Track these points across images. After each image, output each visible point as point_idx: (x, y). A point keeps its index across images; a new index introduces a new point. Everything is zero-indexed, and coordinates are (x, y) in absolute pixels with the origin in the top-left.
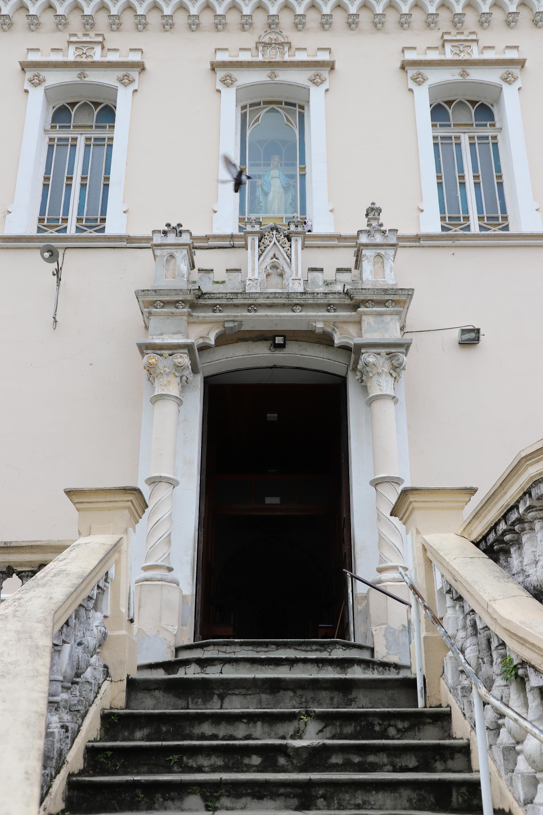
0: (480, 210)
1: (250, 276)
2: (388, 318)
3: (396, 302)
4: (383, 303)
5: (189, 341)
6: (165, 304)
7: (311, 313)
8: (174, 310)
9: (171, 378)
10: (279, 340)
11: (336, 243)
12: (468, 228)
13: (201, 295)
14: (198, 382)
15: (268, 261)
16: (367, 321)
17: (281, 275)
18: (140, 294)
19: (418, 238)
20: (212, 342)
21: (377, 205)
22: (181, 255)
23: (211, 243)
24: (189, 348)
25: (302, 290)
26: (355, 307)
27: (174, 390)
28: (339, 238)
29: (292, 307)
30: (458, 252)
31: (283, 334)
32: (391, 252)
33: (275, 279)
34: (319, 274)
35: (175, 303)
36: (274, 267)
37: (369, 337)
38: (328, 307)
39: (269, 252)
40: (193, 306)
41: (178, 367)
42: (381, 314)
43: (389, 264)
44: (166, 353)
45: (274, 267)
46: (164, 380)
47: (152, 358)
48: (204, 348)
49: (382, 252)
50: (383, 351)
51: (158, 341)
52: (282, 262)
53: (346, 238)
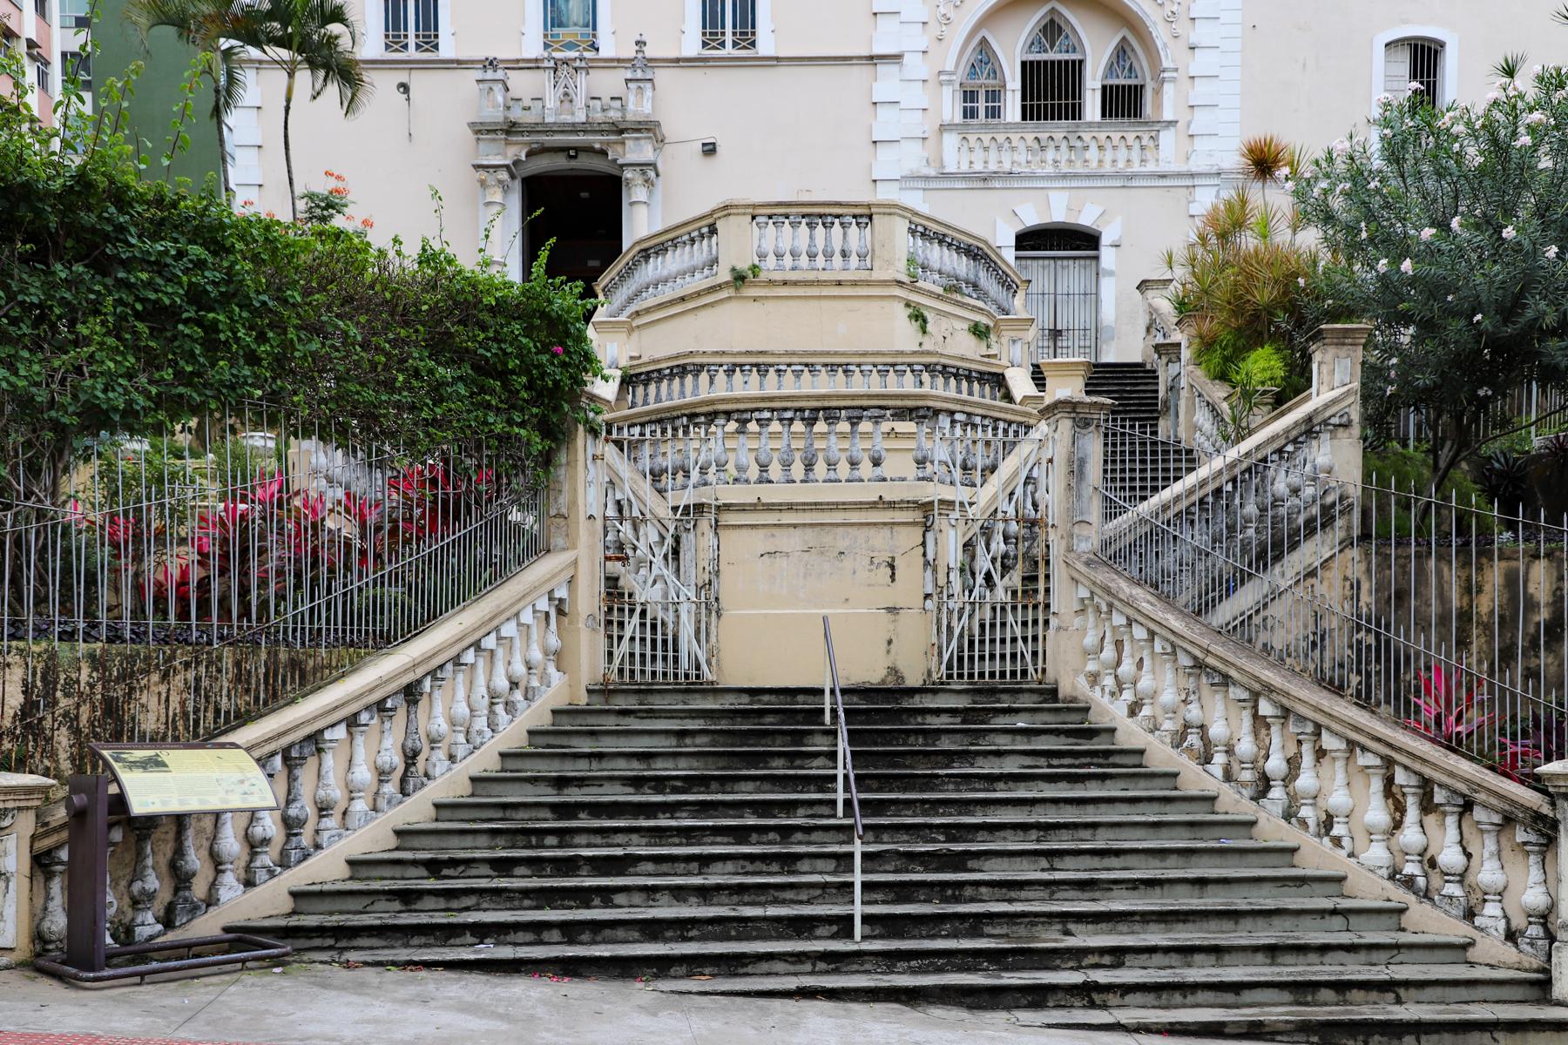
0: (734, 26)
1: (548, 106)
2: (643, 142)
3: (648, 130)
4: (638, 130)
5: (507, 162)
6: (489, 131)
7: (591, 137)
8: (494, 136)
9: (496, 189)
10: (572, 153)
11: (615, 64)
12: (723, 44)
13: (514, 124)
14: (517, 186)
15: (562, 90)
16: (629, 143)
17: (571, 101)
18: (472, 125)
19: (678, 60)
20: (524, 158)
21: (643, 39)
22: (498, 87)
23: (521, 65)
24: (507, 167)
25: (584, 120)
26: (621, 132)
27: (498, 197)
28: (619, 60)
29: (576, 132)
30: (709, 71)
31: (577, 149)
32: (649, 85)
33: (567, 104)
34: (597, 102)
35: (495, 131)
36: (566, 94)
37: (631, 157)
38: (601, 132)
39: (562, 82)
40: (508, 132)
41: (500, 182)
42: (637, 139)
43: (649, 93)
44: (491, 170)
45: (566, 94)
46: (491, 190)
47: (483, 175)
48: (517, 163)
49: (642, 85)
50: (638, 169)
51: (485, 163)
52: (570, 91)
53: (624, 60)
